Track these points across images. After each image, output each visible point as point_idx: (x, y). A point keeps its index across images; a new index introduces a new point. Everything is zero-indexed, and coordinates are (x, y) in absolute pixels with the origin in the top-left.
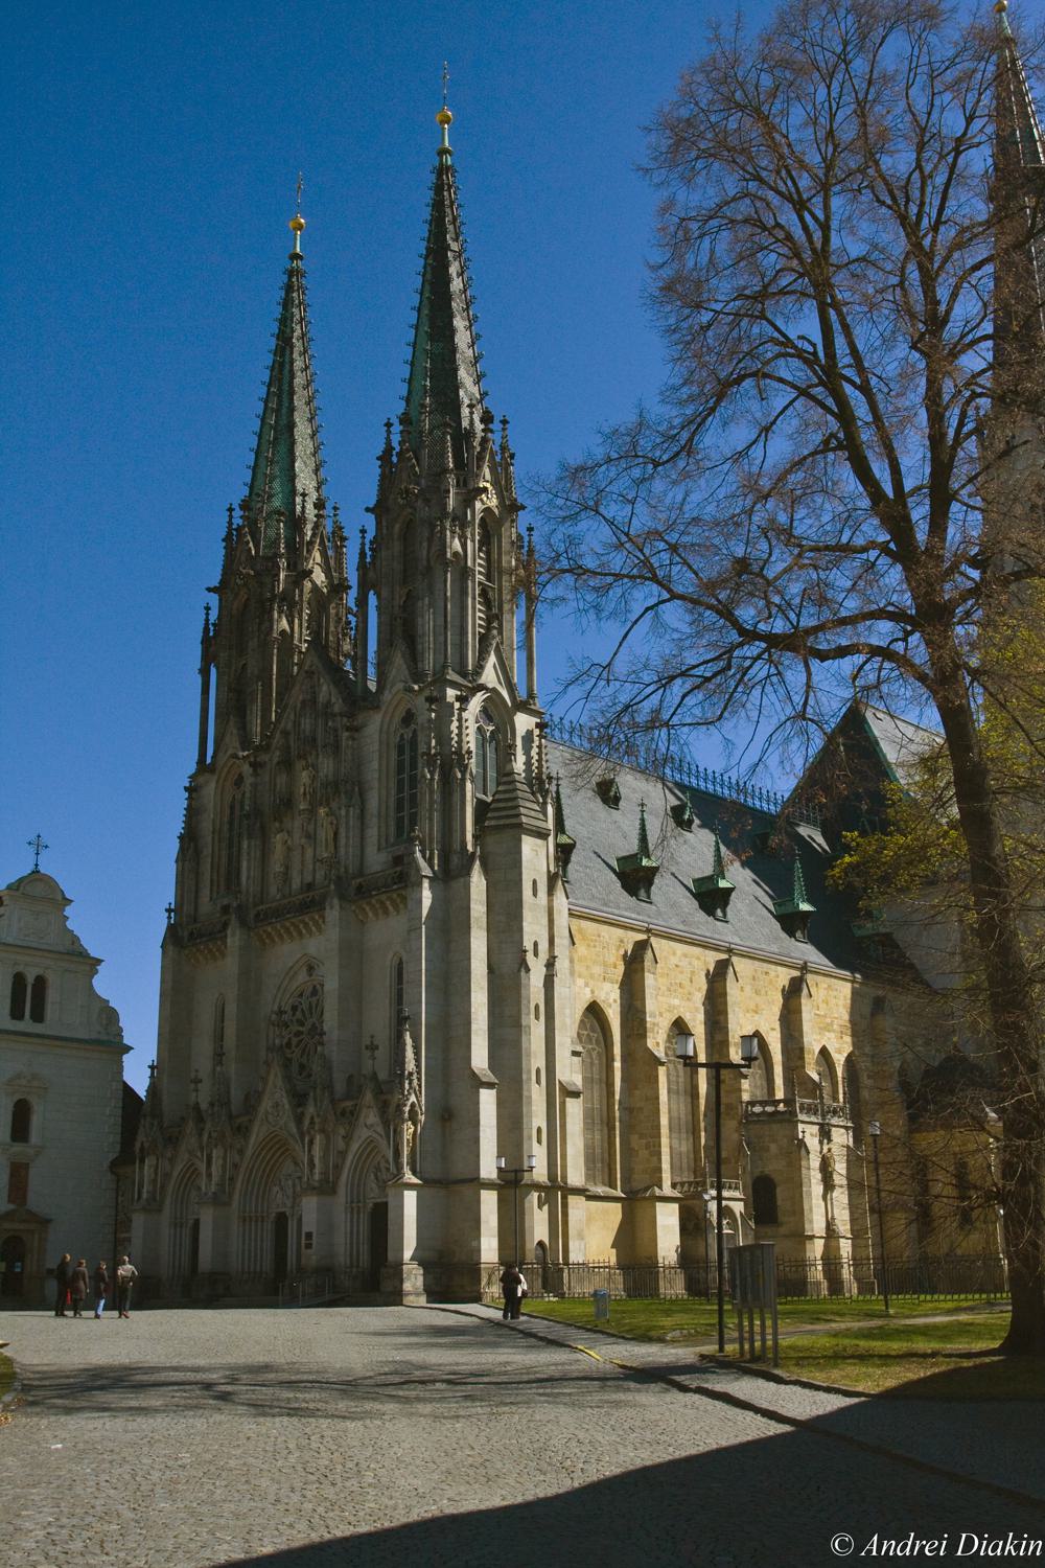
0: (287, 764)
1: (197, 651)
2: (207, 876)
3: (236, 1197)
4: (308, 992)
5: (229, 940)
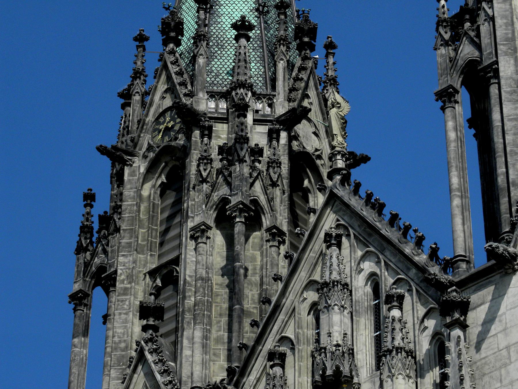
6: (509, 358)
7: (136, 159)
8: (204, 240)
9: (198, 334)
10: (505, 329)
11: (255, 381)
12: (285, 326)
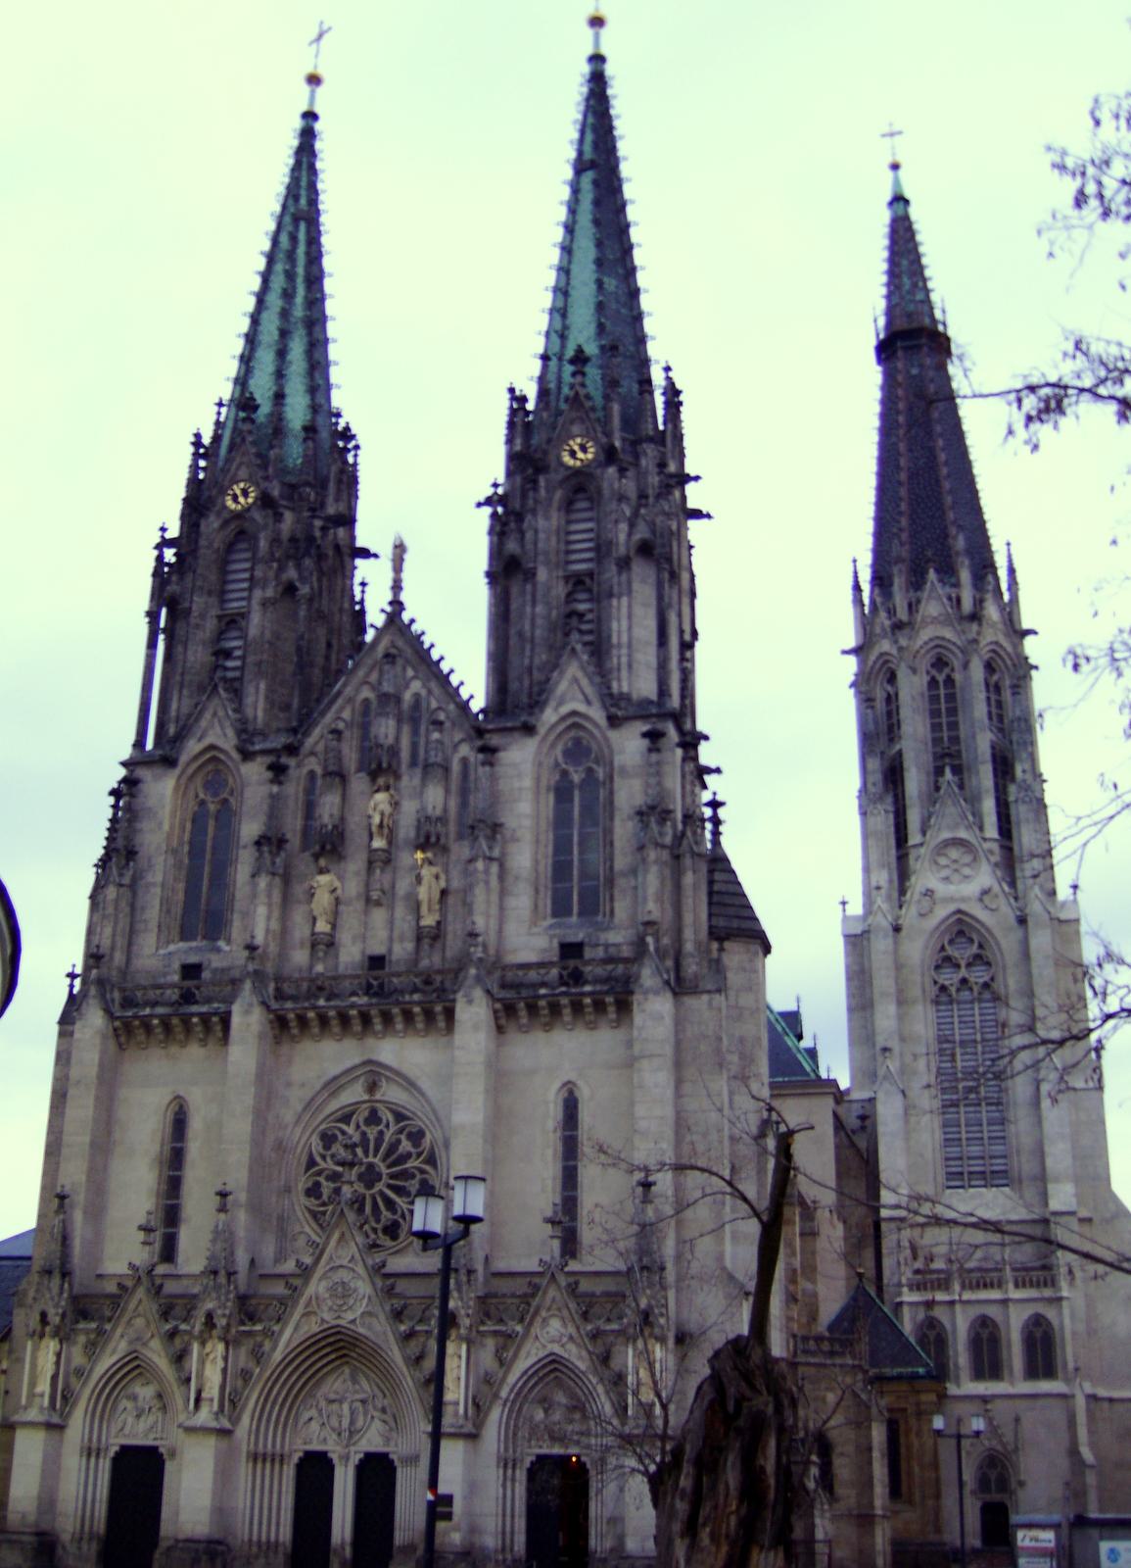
0: (338, 776)
1: (147, 583)
2: (152, 913)
3: (246, 1420)
4: (361, 1116)
5: (236, 1020)
9: (262, 686)
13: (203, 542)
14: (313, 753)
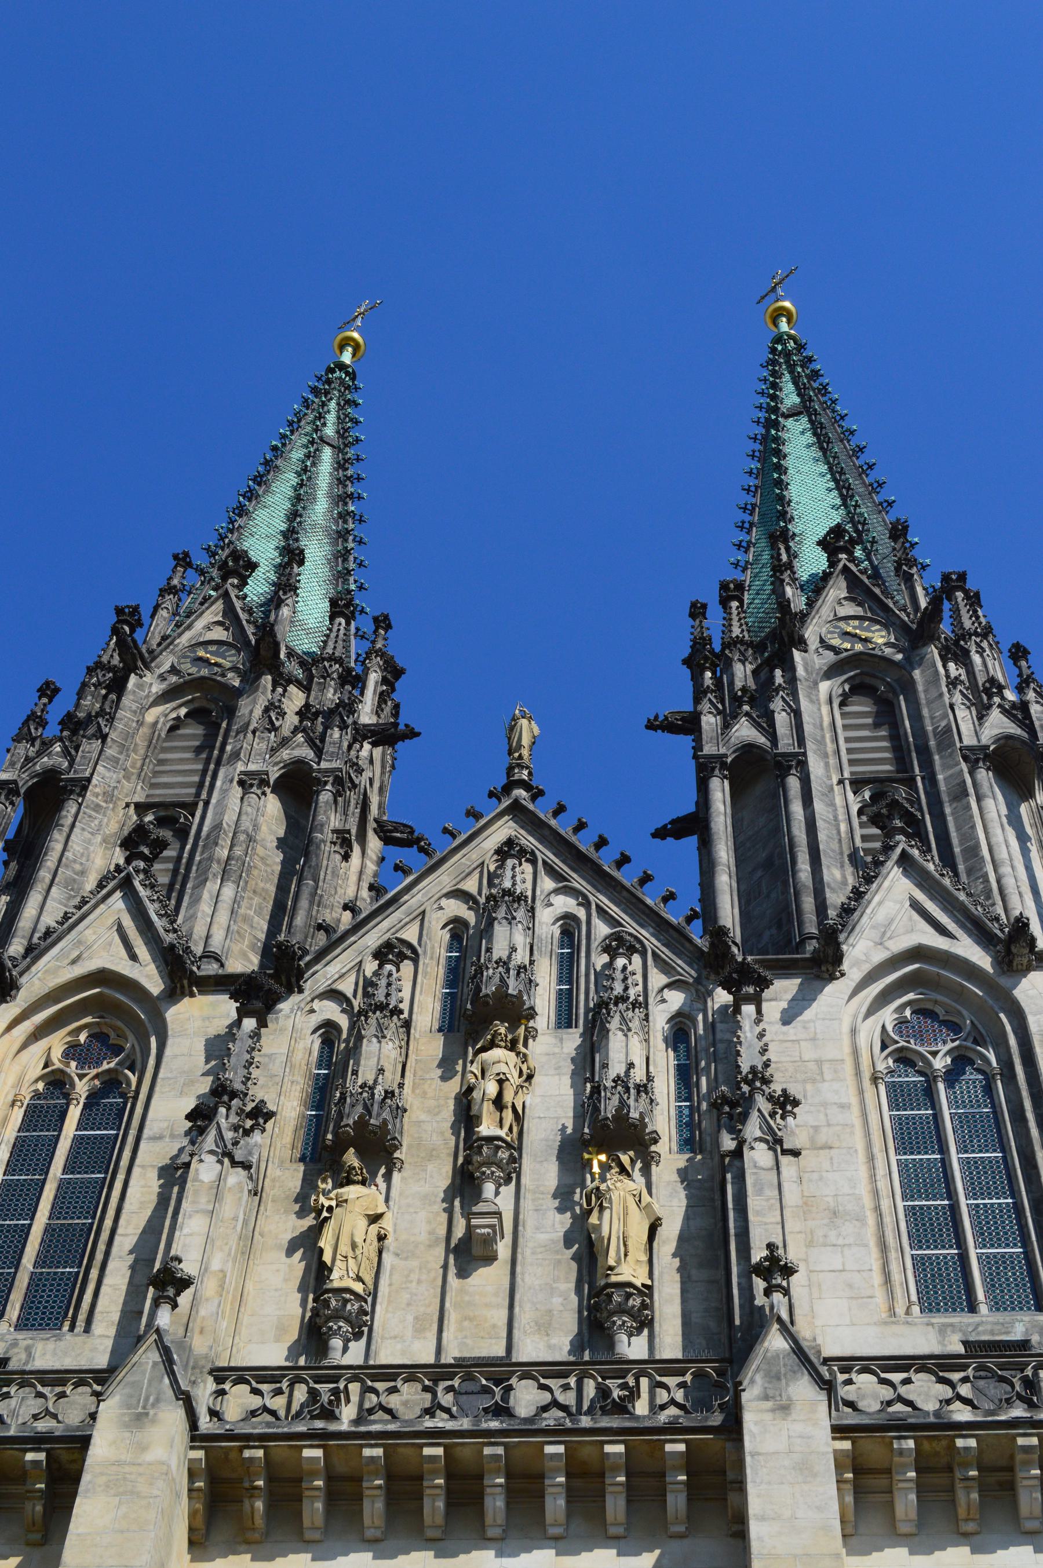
6: (822, 1073)
7: (147, 672)
8: (259, 792)
9: (228, 892)
10: (814, 1039)
11: (337, 976)
12: (402, 927)
13: (126, 701)
14: (333, 994)
